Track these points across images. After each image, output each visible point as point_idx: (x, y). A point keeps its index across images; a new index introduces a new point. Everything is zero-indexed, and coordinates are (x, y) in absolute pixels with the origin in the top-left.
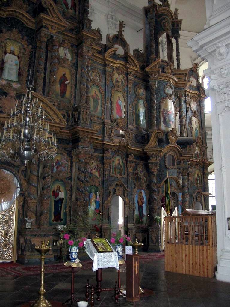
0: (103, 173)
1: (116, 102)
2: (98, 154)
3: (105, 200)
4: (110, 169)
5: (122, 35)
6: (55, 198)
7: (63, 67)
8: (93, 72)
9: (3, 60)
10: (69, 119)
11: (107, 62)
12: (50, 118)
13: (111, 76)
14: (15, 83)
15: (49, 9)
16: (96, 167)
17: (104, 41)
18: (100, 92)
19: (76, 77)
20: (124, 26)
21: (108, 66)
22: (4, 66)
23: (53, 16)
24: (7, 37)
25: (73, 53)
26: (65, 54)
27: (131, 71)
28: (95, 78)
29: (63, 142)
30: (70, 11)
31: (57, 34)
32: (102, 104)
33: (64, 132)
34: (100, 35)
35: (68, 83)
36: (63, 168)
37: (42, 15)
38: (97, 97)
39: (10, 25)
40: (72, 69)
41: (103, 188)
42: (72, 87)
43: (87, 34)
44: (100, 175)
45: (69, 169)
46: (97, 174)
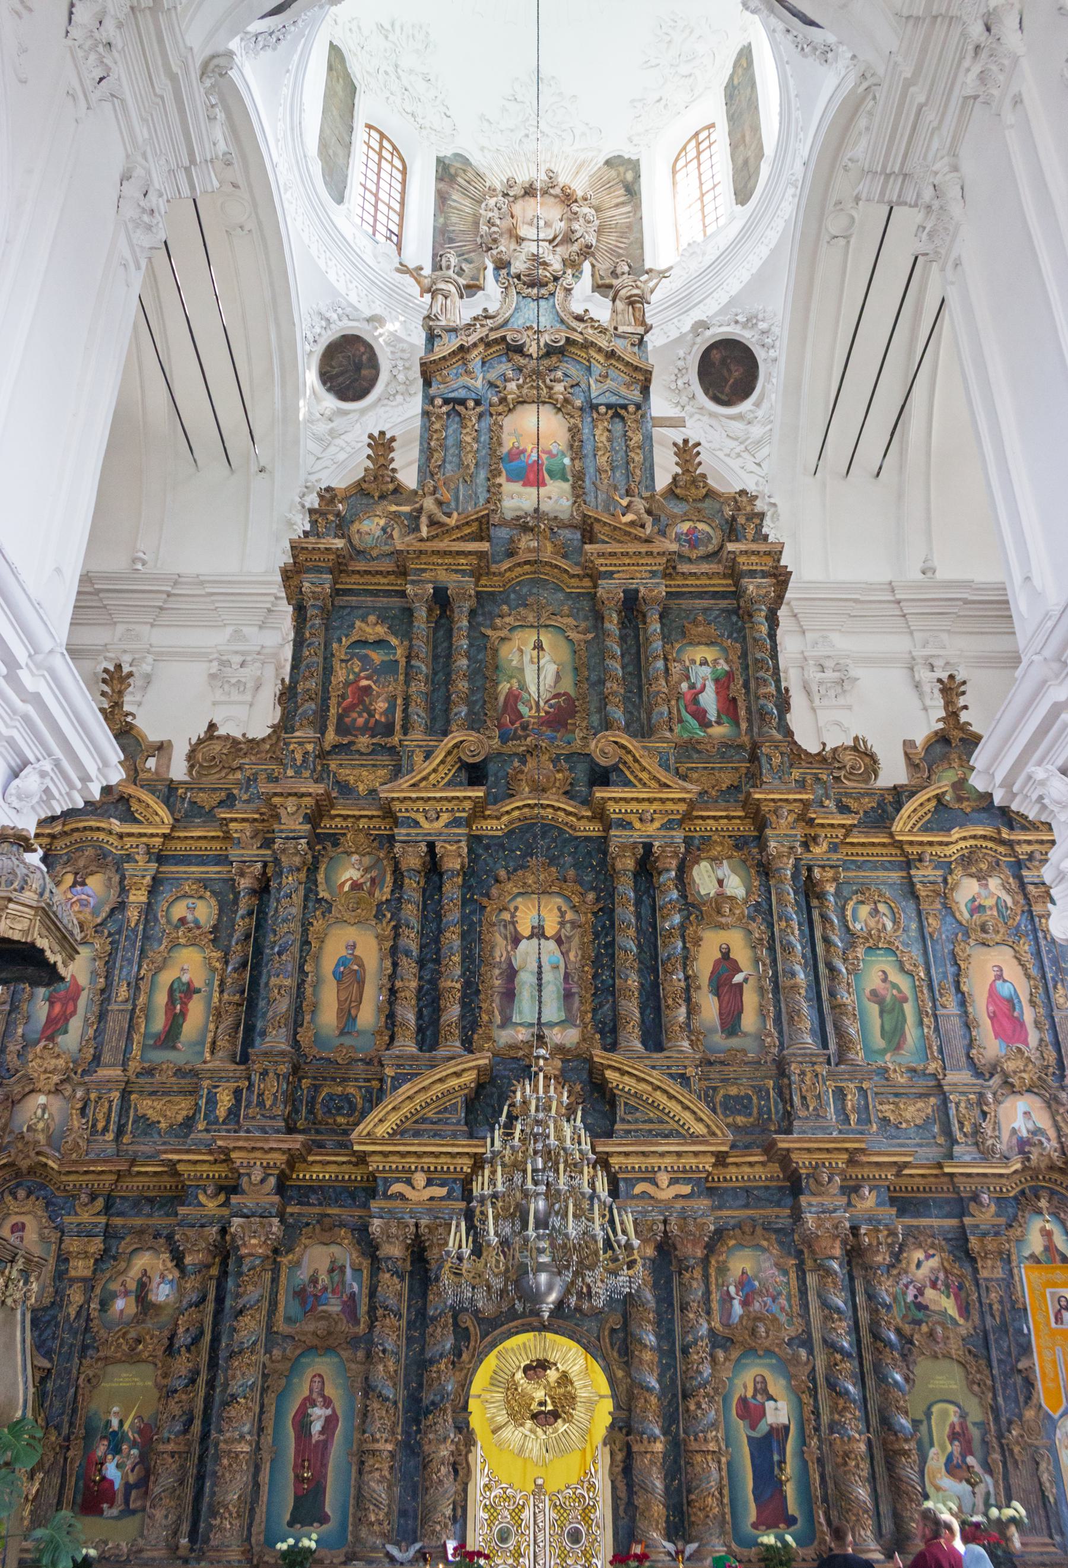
0: (975, 1296)
1: (986, 995)
2: (935, 1222)
3: (1010, 1422)
4: (1012, 1275)
5: (963, 727)
6: (753, 1427)
7: (722, 927)
8: (862, 902)
9: (510, 965)
11: (909, 849)
12: (676, 1126)
13: (944, 895)
14: (556, 1030)
15: (625, 763)
16: (942, 1276)
18: (902, 969)
19: (772, 949)
20: (962, 688)
21: (920, 860)
22: (516, 981)
23: (640, 780)
24: (516, 890)
25: (748, 869)
26: (720, 882)
27: (1028, 848)
28: (872, 923)
29: (759, 1199)
30: (717, 731)
31: (663, 833)
32: (920, 1013)
33: (751, 1164)
34: (867, 760)
35: (746, 980)
36: (769, 1300)
37: (600, 793)
38: (895, 992)
39: (520, 850)
41: (990, 1366)
42: (761, 991)
44: (965, 1310)
45: (795, 1301)
46: (949, 1305)
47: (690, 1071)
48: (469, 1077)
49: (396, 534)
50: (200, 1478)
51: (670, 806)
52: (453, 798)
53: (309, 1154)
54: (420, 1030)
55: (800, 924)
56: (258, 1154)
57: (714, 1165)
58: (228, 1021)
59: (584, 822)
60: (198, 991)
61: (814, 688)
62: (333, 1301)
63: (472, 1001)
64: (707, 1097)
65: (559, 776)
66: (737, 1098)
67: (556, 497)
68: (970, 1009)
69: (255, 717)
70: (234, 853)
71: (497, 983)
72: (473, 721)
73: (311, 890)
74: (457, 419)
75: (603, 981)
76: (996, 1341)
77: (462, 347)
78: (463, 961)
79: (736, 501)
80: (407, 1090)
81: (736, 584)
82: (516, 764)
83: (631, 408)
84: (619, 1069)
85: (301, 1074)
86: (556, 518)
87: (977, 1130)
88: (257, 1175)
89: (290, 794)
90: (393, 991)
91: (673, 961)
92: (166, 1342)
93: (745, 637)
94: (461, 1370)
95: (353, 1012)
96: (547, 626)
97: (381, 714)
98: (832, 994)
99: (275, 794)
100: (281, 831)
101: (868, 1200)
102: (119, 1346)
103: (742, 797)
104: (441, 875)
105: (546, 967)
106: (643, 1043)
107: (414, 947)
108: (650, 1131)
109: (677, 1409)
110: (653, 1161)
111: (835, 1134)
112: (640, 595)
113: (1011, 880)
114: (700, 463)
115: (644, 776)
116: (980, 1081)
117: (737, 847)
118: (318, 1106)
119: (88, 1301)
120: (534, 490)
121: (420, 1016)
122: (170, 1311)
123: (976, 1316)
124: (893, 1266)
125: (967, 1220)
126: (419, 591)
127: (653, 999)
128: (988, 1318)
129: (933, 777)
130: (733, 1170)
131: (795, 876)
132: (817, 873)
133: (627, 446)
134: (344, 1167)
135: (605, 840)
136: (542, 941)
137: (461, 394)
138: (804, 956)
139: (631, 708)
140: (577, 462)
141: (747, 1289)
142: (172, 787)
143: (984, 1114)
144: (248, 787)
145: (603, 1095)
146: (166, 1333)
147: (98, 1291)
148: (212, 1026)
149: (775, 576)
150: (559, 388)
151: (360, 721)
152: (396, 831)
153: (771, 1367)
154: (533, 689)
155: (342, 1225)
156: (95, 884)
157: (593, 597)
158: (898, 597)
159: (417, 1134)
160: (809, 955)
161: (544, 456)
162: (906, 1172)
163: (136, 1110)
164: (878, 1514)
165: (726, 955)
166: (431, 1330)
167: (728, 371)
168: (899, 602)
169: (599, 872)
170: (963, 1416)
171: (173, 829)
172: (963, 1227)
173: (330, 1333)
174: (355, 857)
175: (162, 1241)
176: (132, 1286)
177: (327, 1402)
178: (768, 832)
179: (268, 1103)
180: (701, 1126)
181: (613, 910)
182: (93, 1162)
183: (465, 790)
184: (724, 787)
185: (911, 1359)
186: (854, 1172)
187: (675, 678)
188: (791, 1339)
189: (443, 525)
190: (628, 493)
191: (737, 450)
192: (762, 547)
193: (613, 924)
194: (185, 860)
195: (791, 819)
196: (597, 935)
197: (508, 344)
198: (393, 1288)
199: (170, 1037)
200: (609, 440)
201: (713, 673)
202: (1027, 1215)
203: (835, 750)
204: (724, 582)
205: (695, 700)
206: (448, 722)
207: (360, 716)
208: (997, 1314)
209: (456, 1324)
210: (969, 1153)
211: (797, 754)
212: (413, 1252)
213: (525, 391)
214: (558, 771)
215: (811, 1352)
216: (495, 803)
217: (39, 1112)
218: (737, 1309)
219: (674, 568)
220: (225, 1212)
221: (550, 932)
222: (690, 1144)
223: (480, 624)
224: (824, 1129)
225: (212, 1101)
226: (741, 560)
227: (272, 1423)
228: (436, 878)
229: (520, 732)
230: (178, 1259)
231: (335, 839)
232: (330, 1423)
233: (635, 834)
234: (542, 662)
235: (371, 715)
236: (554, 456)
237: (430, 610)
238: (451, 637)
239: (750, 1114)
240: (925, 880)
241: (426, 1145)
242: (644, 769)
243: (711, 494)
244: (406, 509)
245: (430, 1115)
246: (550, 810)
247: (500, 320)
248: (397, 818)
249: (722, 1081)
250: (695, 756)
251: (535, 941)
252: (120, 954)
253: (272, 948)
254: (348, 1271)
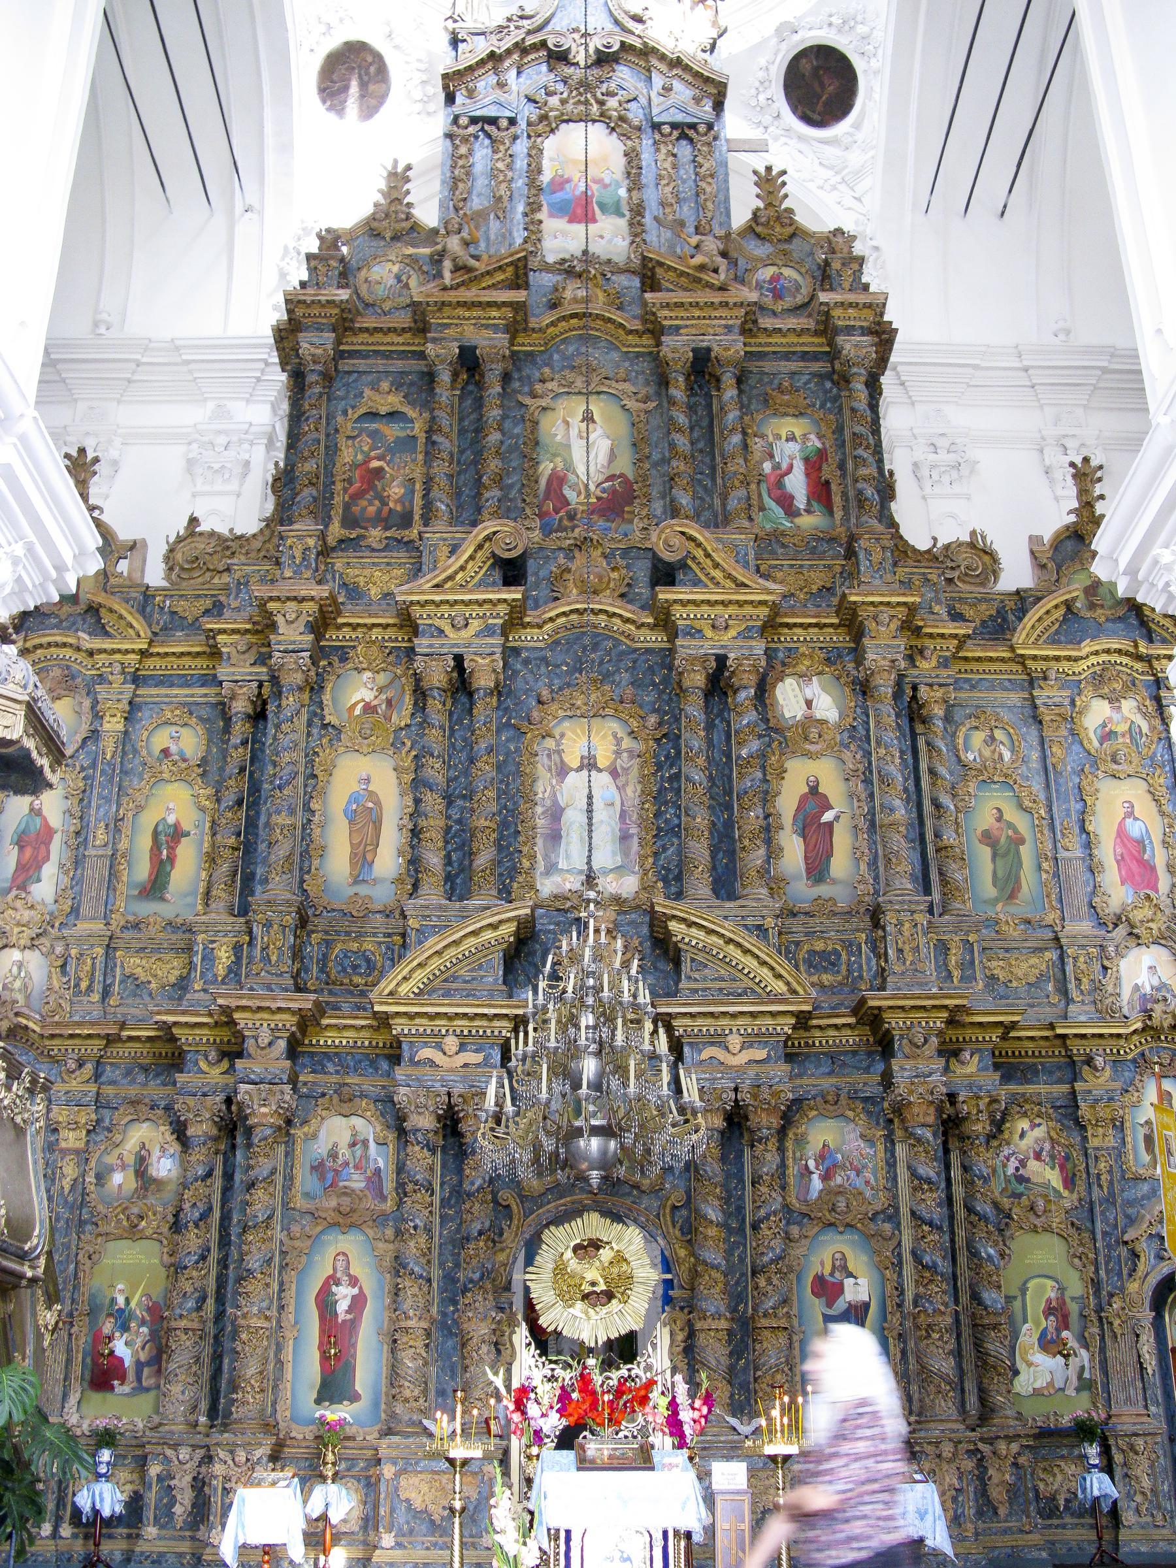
1: (1114, 835)
2: (1043, 1089)
3: (1111, 1295)
6: (830, 1305)
8: (976, 728)
9: (555, 803)
10: (861, 967)
13: (1071, 719)
15: (694, 558)
16: (1047, 1146)
17: (1017, 573)
18: (1020, 806)
20: (1099, 474)
21: (1045, 678)
26: (809, 704)
28: (987, 753)
32: (1040, 857)
33: (836, 1027)
34: (986, 558)
35: (837, 818)
36: (853, 1174)
37: (665, 594)
38: (1010, 832)
39: (567, 665)
40: (847, 755)
41: (1095, 1240)
43: (871, 599)
44: (1069, 1182)
46: (1054, 1177)
47: (770, 922)
48: (507, 931)
49: (413, 283)
50: (217, 1357)
51: (748, 610)
52: (485, 601)
53: (323, 1014)
54: (449, 878)
55: (902, 752)
56: (266, 1016)
57: (794, 1028)
58: (225, 867)
59: (644, 631)
60: (188, 834)
61: (925, 472)
62: (355, 1177)
63: (510, 845)
64: (787, 950)
65: (615, 575)
66: (823, 954)
67: (610, 238)
68: (1095, 852)
69: (240, 509)
70: (223, 672)
71: (540, 822)
72: (509, 509)
73: (316, 714)
74: (487, 142)
75: (666, 821)
76: (1103, 1213)
77: (492, 55)
78: (499, 798)
79: (830, 242)
80: (434, 943)
81: (831, 343)
82: (562, 561)
83: (702, 128)
84: (684, 920)
85: (310, 927)
86: (609, 261)
87: (1097, 987)
88: (264, 1040)
89: (288, 599)
90: (416, 833)
91: (751, 794)
92: (171, 1219)
93: (840, 409)
94: (502, 1250)
95: (369, 857)
96: (599, 393)
97: (396, 502)
98: (937, 835)
99: (271, 599)
100: (279, 643)
101: (970, 1067)
102: (119, 1221)
103: (835, 601)
104: (470, 694)
105: (598, 804)
106: (714, 890)
107: (440, 779)
108: (721, 990)
109: (746, 1287)
110: (724, 1022)
111: (934, 990)
112: (713, 355)
113: (1148, 703)
114: (786, 196)
115: (717, 574)
116: (1103, 932)
117: (828, 661)
118: (331, 964)
119: (83, 1174)
120: (582, 227)
121: (448, 861)
122: (172, 1187)
123: (1081, 1186)
124: (994, 1137)
125: (1079, 1086)
126: (442, 351)
127: (725, 843)
128: (1095, 1188)
129: (1064, 580)
130: (817, 1033)
131: (897, 695)
132: (923, 692)
133: (697, 174)
134: (363, 1034)
135: (672, 651)
136: (593, 773)
137: (491, 112)
138: (906, 790)
139: (701, 493)
140: (634, 193)
141: (827, 1163)
142: (147, 594)
143: (1105, 968)
144: (239, 591)
145: (666, 952)
146: (171, 1209)
147: (93, 1164)
148: (204, 874)
149: (877, 333)
150: (612, 103)
151: (372, 510)
152: (416, 641)
153: (853, 1242)
154: (581, 470)
155: (363, 1096)
157: (655, 358)
158: (1026, 363)
159: (447, 994)
160: (912, 788)
161: (595, 187)
162: (1013, 1034)
163: (122, 966)
164: (963, 1391)
165: (814, 790)
166: (467, 1206)
167: (821, 84)
168: (1026, 370)
169: (664, 691)
170: (1062, 1289)
171: (150, 644)
172: (1073, 1093)
173: (353, 1210)
174: (368, 674)
175: (160, 1112)
176: (130, 1159)
177: (354, 1281)
178: (866, 641)
179: (274, 958)
180: (781, 984)
181: (679, 737)
182: (79, 1024)
183: (498, 592)
184: (814, 588)
185: (1008, 1233)
186: (952, 1034)
187: (757, 456)
188: (876, 1214)
189: (468, 269)
190: (698, 230)
191: (832, 182)
192: (862, 299)
193: (678, 753)
194: (164, 681)
195: (895, 624)
196: (659, 766)
197: (549, 50)
198: (421, 1160)
199: (155, 888)
200: (674, 167)
201: (801, 450)
202: (1145, 1078)
203: (947, 547)
204: (816, 340)
205: (779, 484)
206: (479, 510)
207: (371, 504)
208: (1105, 1185)
209: (495, 1201)
210: (1087, 1013)
211: (902, 550)
212: (445, 1126)
213: (570, 107)
214: (613, 569)
215: (898, 1225)
216: (536, 607)
217: (15, 970)
218: (817, 1184)
219: (755, 322)
220: (229, 1079)
221: (602, 762)
222: (762, 1003)
223: (515, 392)
224: (921, 985)
225: (209, 958)
226: (836, 313)
227: (292, 1301)
228: (464, 699)
229: (566, 523)
230: (180, 1132)
231: (343, 654)
232: (358, 1303)
233: (707, 644)
234: (592, 437)
235: (384, 503)
236: (605, 186)
237: (455, 375)
238: (481, 407)
239: (838, 972)
240: (1050, 702)
241: (458, 1005)
242: (716, 566)
243: (797, 233)
244: (426, 251)
245: (462, 972)
246: (603, 617)
247: (538, 21)
248: (417, 626)
249: (807, 934)
250: (780, 551)
251: (585, 773)
252: (95, 792)
253: (271, 783)
254: (372, 1145)
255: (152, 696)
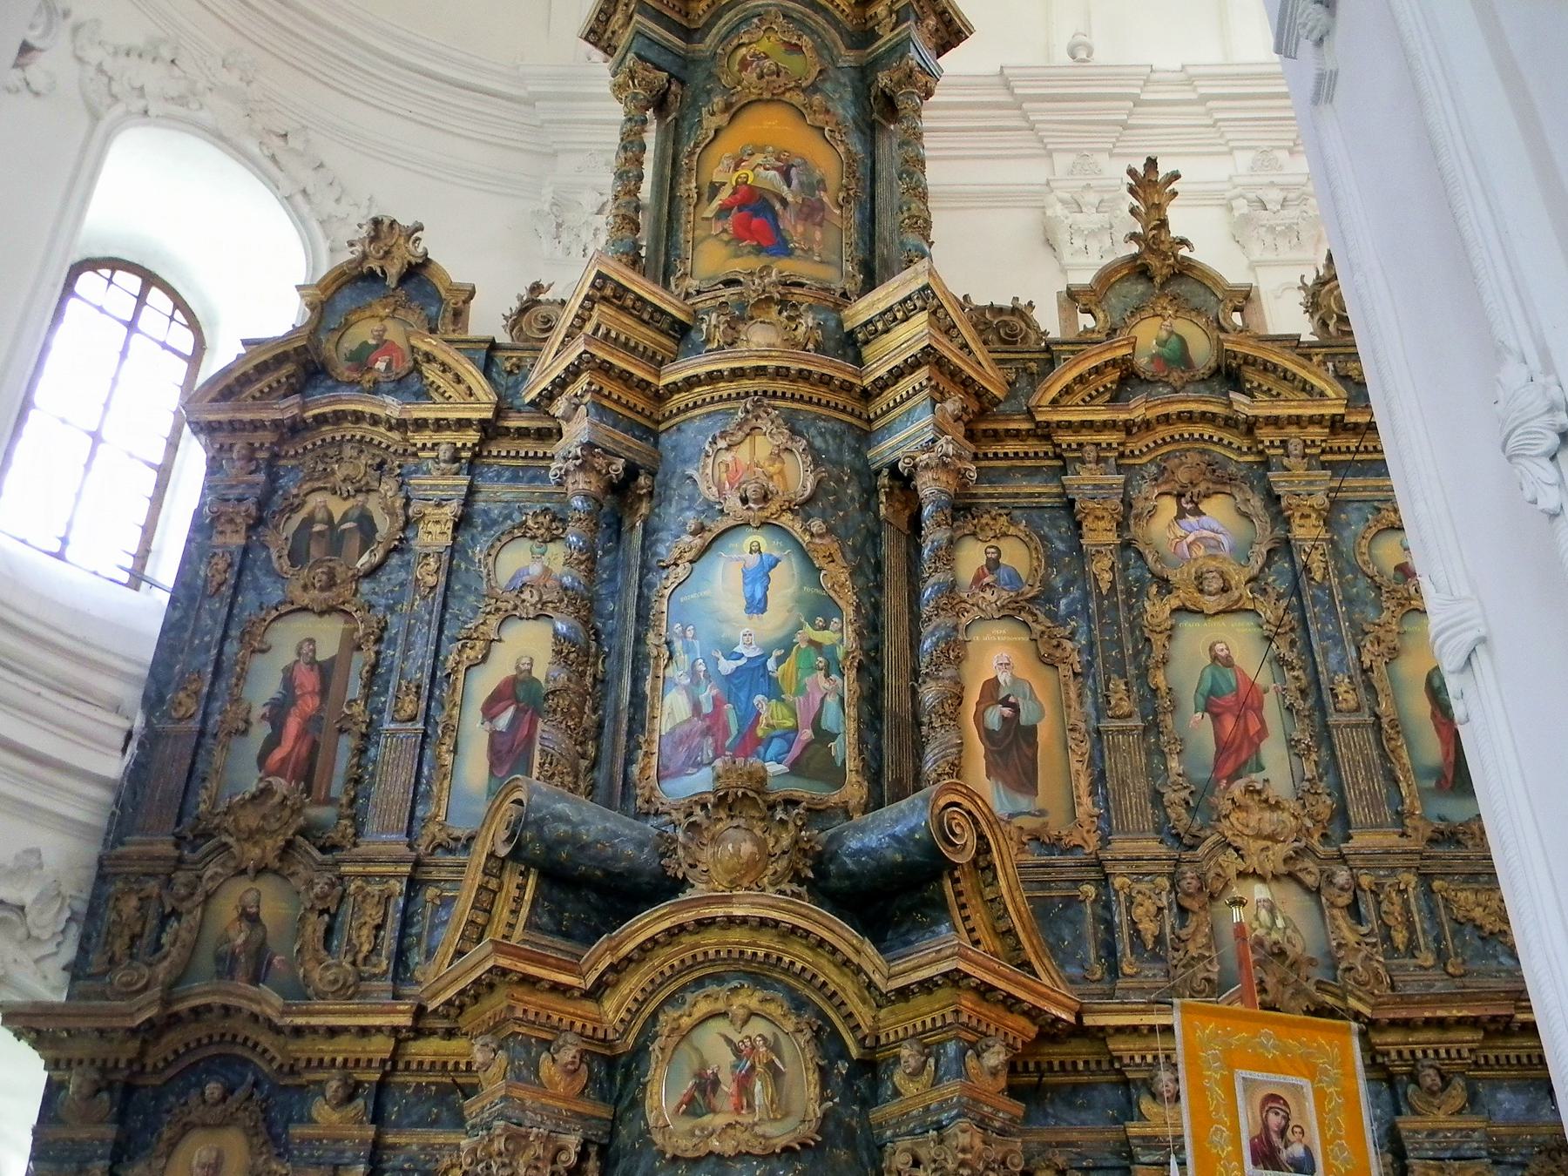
156: (1218, 511)
217: (1264, 915)
255: (1355, 490)
